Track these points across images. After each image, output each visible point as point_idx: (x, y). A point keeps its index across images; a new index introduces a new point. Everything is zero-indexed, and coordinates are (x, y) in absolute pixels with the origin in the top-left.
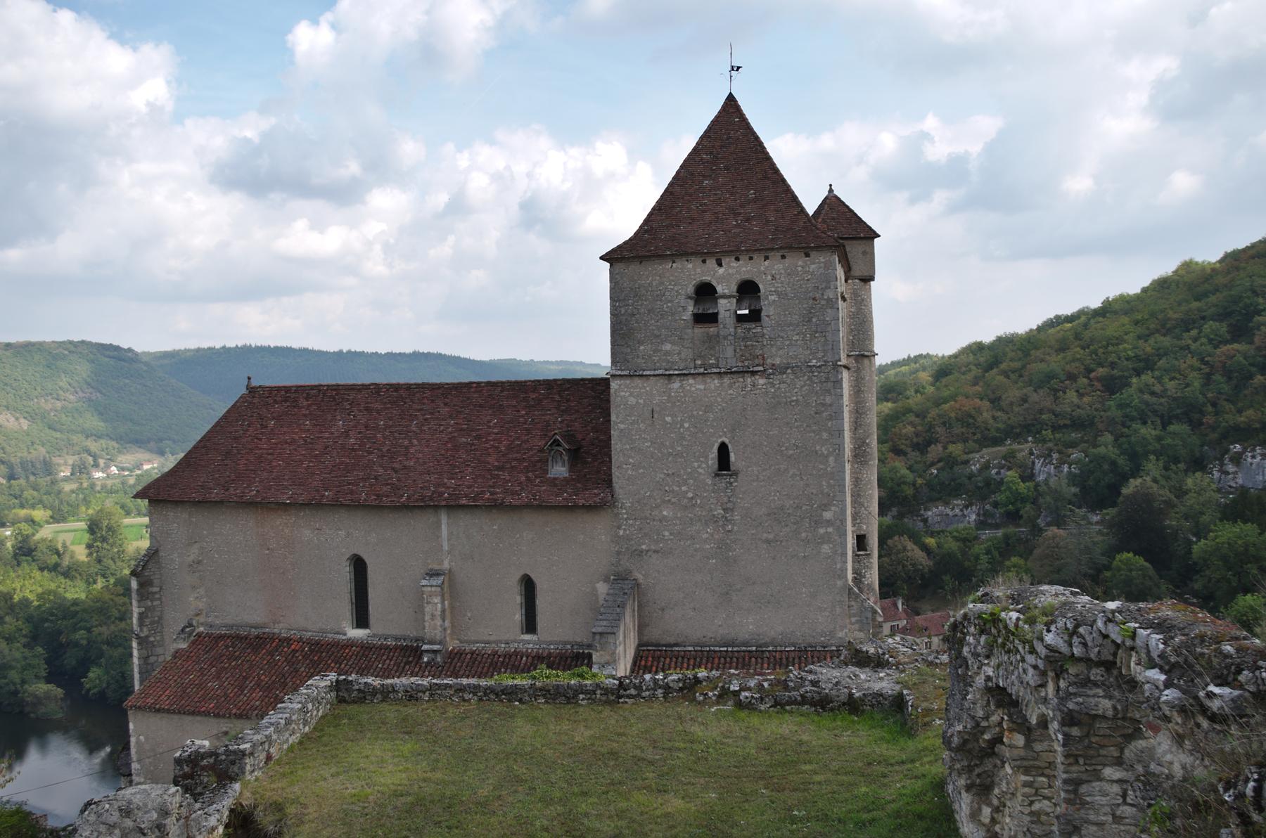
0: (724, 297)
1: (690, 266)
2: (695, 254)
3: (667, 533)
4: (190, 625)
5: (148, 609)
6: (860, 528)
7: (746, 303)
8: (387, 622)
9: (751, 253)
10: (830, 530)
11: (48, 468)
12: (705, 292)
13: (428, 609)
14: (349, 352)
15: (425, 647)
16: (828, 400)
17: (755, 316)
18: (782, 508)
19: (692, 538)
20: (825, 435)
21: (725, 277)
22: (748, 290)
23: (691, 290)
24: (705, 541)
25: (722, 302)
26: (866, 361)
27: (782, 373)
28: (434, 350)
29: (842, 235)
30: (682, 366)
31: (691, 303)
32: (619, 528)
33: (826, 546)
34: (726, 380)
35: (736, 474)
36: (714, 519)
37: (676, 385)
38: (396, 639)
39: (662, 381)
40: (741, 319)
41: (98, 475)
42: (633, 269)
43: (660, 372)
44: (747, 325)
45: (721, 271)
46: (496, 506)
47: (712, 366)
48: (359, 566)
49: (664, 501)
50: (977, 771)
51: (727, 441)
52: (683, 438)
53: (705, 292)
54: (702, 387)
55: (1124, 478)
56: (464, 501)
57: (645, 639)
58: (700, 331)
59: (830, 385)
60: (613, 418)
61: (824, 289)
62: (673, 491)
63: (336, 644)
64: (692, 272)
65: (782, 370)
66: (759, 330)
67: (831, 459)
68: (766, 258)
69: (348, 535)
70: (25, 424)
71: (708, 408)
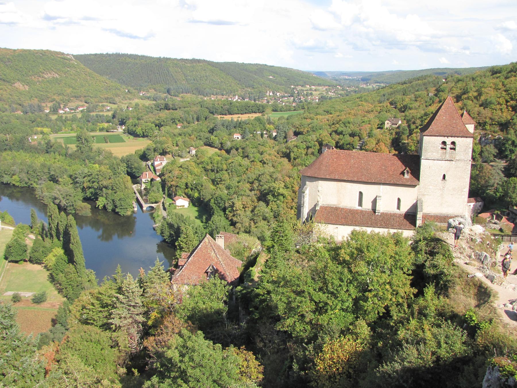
9: (454, 137)
11: (40, 109)
12: (444, 143)
14: (164, 58)
17: (454, 149)
21: (449, 140)
22: (453, 143)
28: (202, 58)
36: (441, 189)
41: (61, 112)
48: (361, 193)
53: (444, 143)
63: (353, 210)
70: (27, 88)
71: (442, 167)
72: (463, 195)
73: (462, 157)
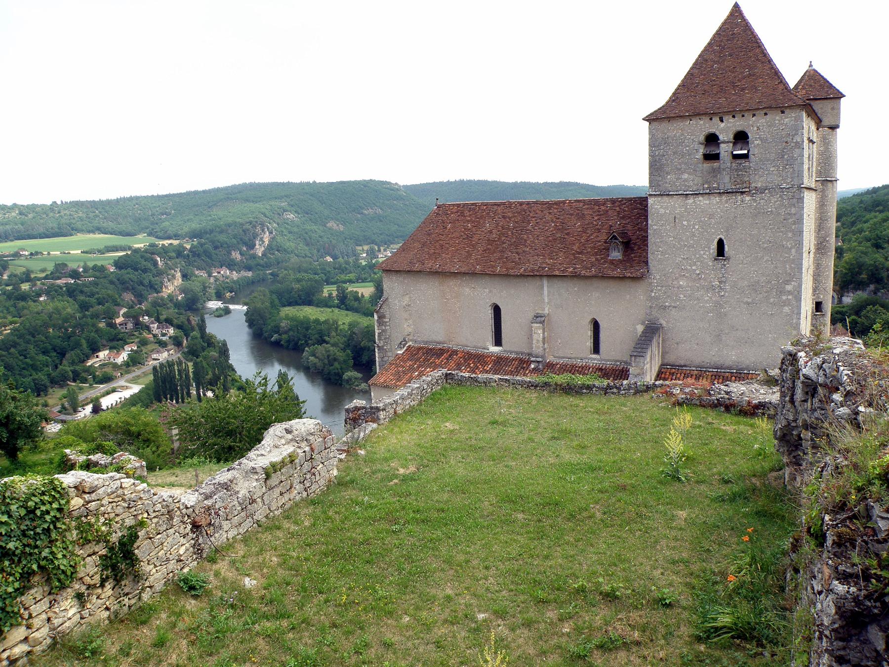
0: (724, 142)
1: (702, 122)
2: (705, 114)
3: (682, 296)
4: (405, 340)
5: (383, 331)
6: (819, 298)
7: (739, 146)
8: (513, 342)
9: (743, 113)
10: (790, 297)
12: (712, 139)
13: (535, 337)
15: (532, 359)
16: (793, 210)
18: (758, 282)
19: (698, 299)
20: (790, 235)
21: (725, 129)
22: (741, 137)
23: (702, 138)
24: (706, 302)
25: (722, 146)
26: (830, 184)
27: (761, 193)
29: (818, 97)
30: (695, 188)
31: (702, 147)
32: (652, 291)
33: (786, 308)
34: (724, 198)
35: (728, 259)
37: (690, 201)
38: (517, 353)
39: (681, 198)
40: (736, 157)
42: (665, 125)
43: (680, 192)
44: (739, 161)
45: (722, 125)
46: (576, 276)
47: (714, 188)
48: (497, 310)
49: (681, 276)
50: (793, 454)
51: (723, 238)
52: (694, 235)
53: (712, 139)
54: (707, 202)
56: (557, 273)
57: (666, 361)
58: (707, 165)
59: (795, 200)
60: (650, 222)
61: (793, 136)
62: (686, 269)
64: (702, 127)
65: (761, 191)
66: (747, 164)
67: (793, 250)
68: (754, 115)
69: (490, 292)
70: (341, 228)
71: (711, 216)
73: (777, 180)
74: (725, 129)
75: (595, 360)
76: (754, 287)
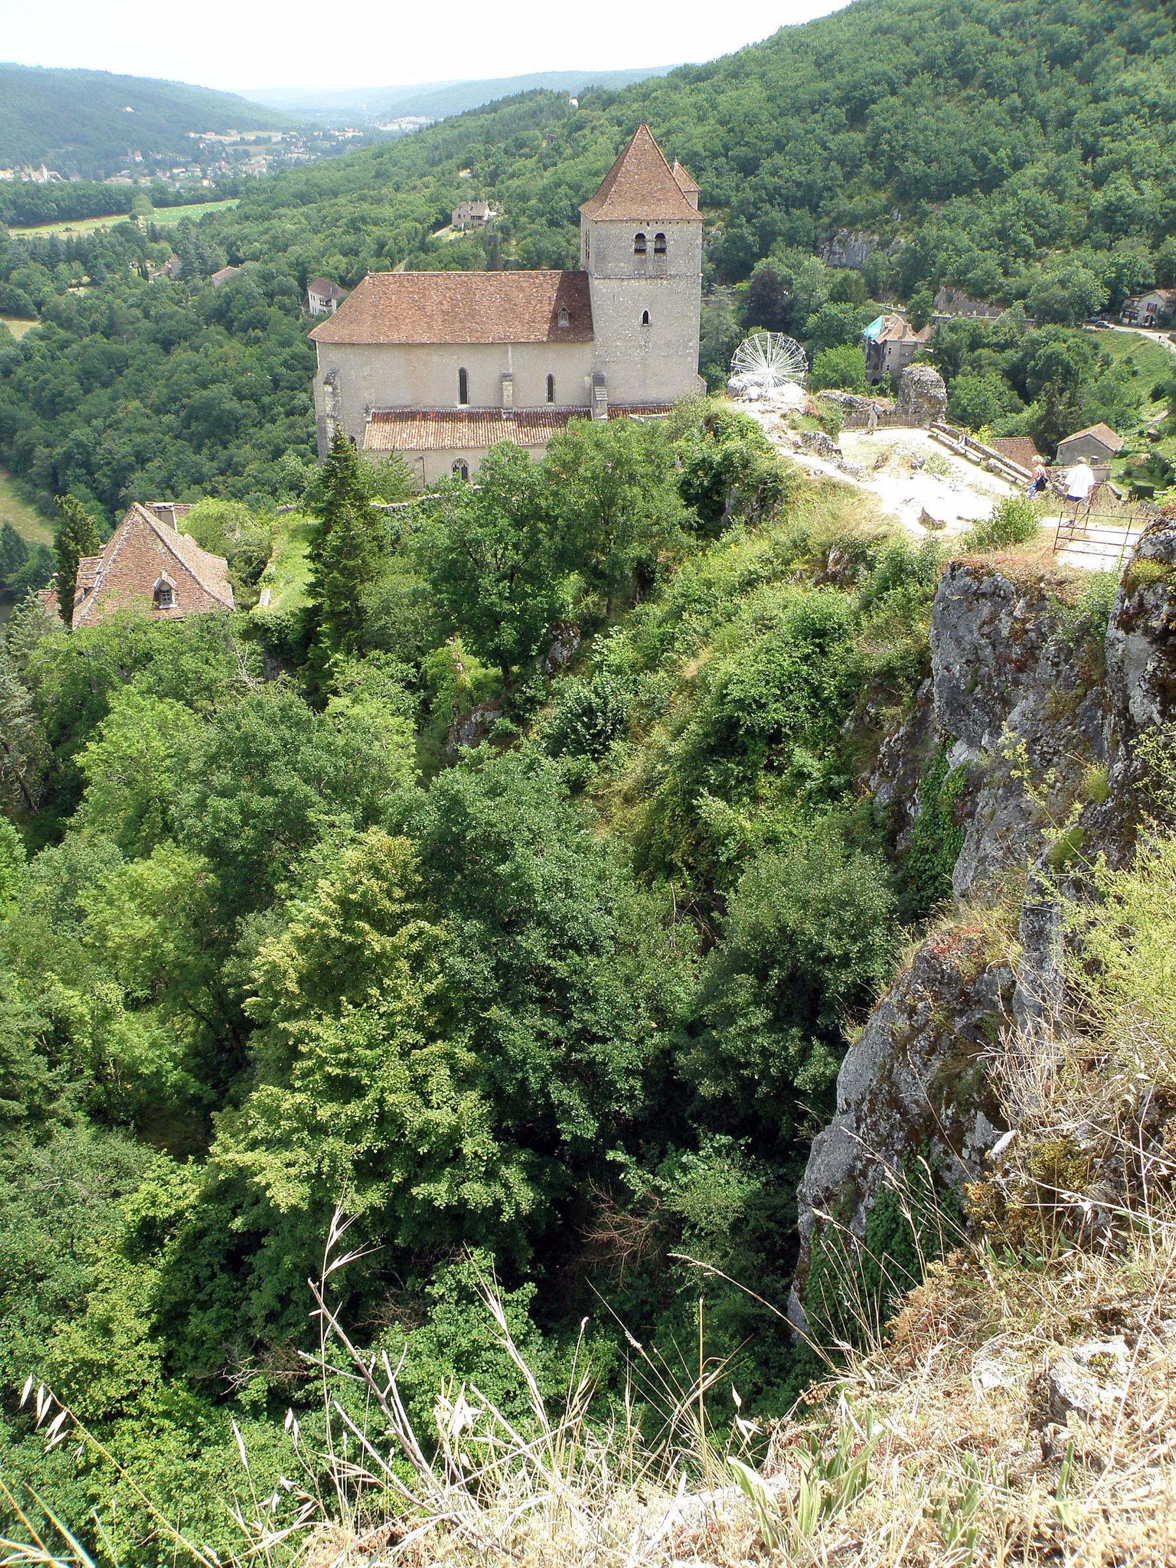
12: (640, 237)
22: (660, 237)
48: (463, 375)
53: (640, 237)
55: (758, 257)
58: (637, 257)
65: (673, 277)
72: (690, 355)
74: (650, 233)
75: (551, 407)
76: (668, 344)
